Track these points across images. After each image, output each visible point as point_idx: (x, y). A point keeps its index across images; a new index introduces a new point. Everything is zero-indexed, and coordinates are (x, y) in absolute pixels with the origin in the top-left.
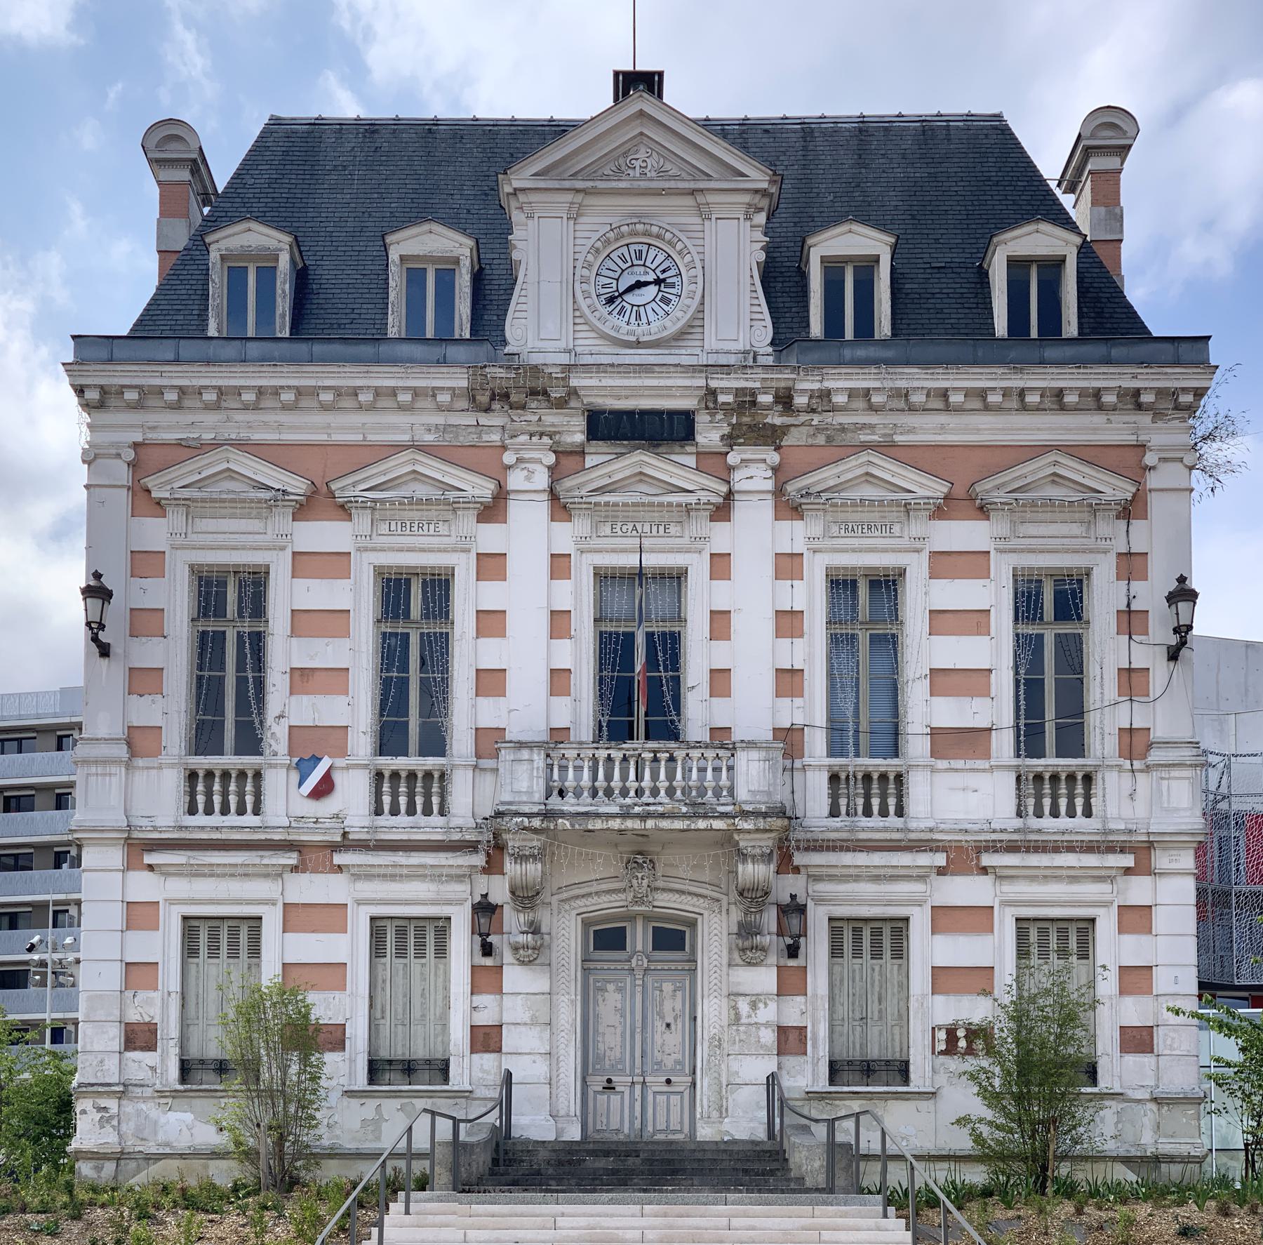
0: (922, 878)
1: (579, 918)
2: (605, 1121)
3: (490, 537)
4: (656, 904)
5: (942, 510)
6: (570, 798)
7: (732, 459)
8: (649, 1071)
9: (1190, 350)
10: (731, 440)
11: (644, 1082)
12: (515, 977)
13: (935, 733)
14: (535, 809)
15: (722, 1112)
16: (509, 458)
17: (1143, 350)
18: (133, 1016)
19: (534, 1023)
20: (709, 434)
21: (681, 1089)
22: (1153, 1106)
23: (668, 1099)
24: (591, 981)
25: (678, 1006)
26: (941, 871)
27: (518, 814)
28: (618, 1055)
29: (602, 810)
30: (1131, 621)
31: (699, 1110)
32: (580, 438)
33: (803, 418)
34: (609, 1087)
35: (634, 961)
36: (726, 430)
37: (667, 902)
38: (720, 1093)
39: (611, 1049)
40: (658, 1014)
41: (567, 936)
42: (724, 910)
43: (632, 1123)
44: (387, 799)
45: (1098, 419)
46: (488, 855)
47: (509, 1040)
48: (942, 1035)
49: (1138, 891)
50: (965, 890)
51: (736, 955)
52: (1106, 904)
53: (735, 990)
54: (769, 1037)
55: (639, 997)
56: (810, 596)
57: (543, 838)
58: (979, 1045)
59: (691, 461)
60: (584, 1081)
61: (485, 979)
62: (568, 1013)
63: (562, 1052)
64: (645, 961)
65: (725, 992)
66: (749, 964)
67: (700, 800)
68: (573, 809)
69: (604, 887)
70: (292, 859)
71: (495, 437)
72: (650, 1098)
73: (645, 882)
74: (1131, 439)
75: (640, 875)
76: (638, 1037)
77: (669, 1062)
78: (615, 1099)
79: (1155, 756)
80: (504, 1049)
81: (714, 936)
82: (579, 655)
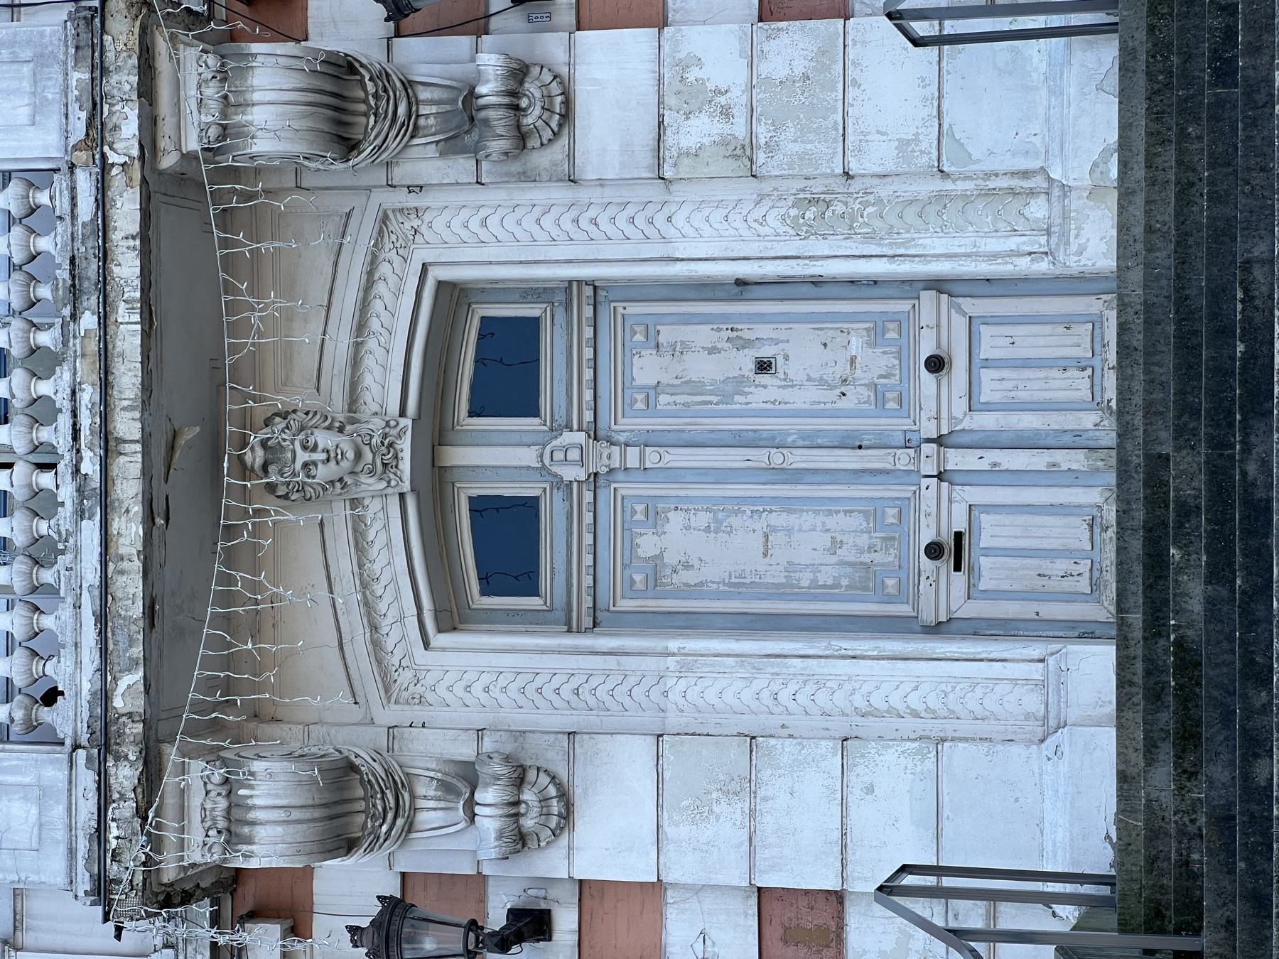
1: (439, 640)
2: (1062, 566)
4: (394, 407)
6: (58, 671)
8: (906, 424)
11: (939, 441)
14: (87, 779)
15: (1030, 183)
19: (749, 786)
21: (960, 324)
23: (987, 364)
24: (626, 604)
25: (702, 335)
27: (100, 832)
28: (856, 521)
29: (91, 576)
31: (1024, 265)
34: (953, 551)
35: (572, 473)
37: (388, 380)
38: (966, 198)
39: (836, 545)
40: (727, 398)
41: (480, 681)
42: (412, 201)
43: (1074, 478)
46: (255, 915)
51: (542, 159)
53: (645, 158)
55: (677, 458)
57: (172, 754)
60: (937, 629)
62: (718, 678)
63: (839, 699)
64: (567, 438)
65: (655, 192)
66: (567, 116)
67: (63, 274)
68: (90, 658)
69: (344, 565)
72: (986, 421)
73: (324, 439)
75: (302, 457)
76: (798, 459)
77: (876, 362)
78: (990, 533)
80: (832, 884)
81: (484, 230)
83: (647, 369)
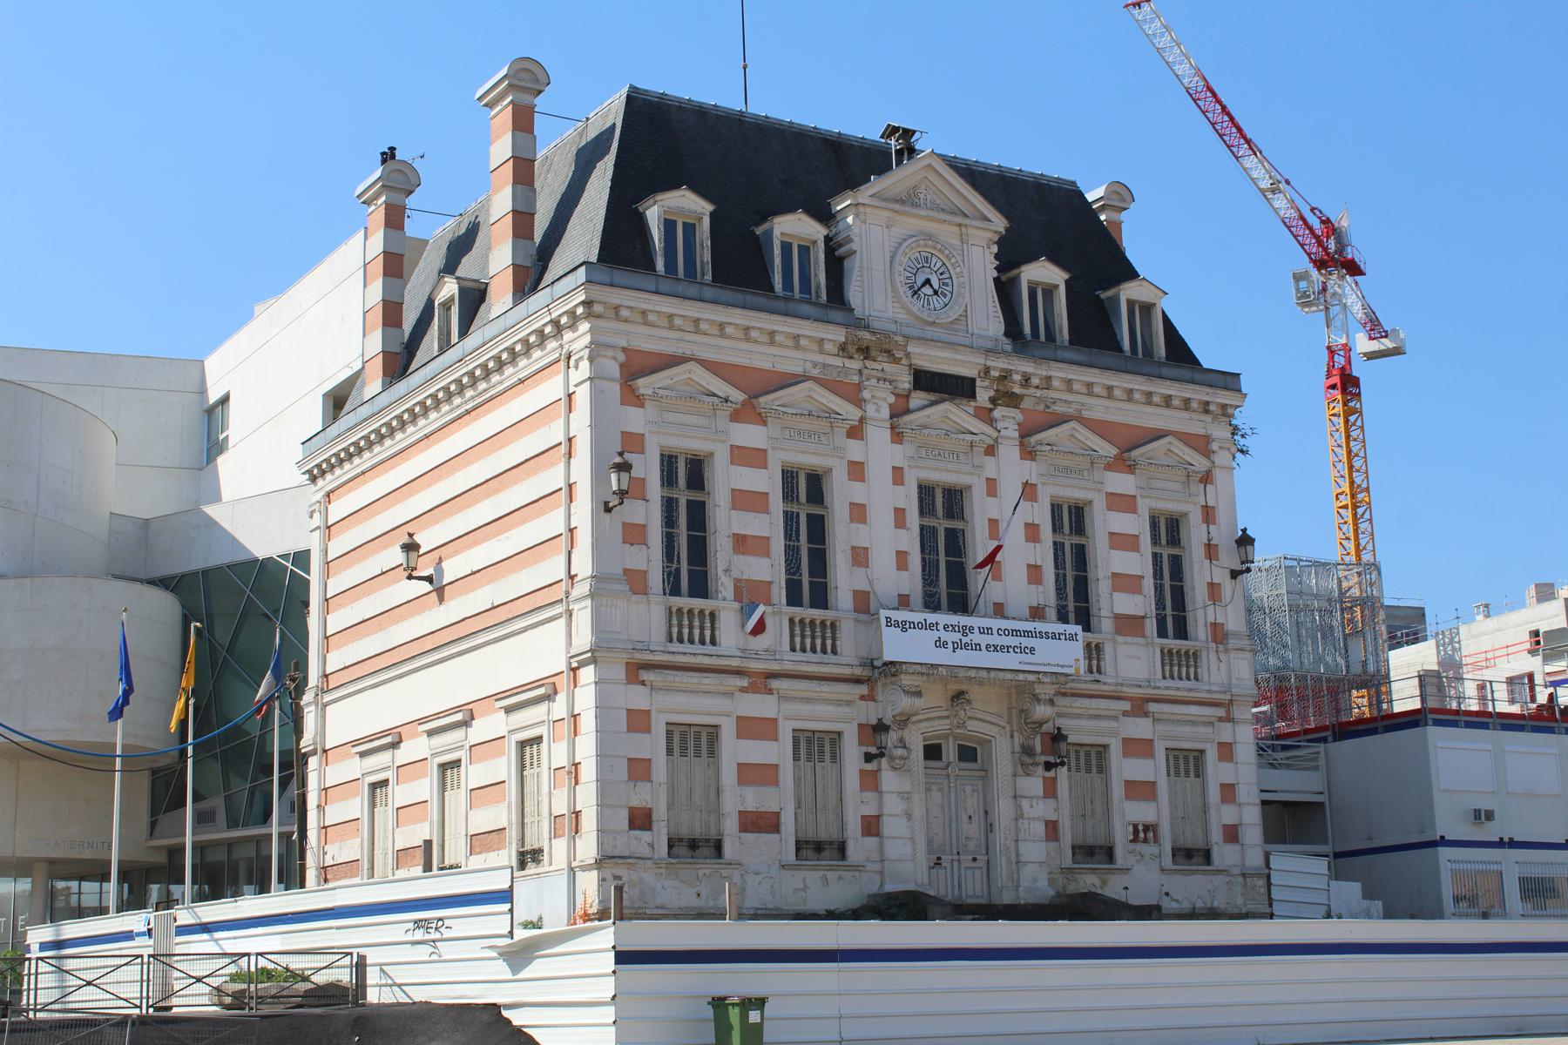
0: (1115, 718)
3: (854, 450)
5: (1112, 466)
7: (997, 413)
9: (1229, 381)
10: (993, 400)
12: (889, 780)
13: (1117, 617)
16: (866, 394)
17: (1198, 376)
18: (635, 803)
20: (983, 395)
22: (1240, 879)
26: (1125, 714)
30: (1211, 551)
32: (907, 386)
33: (1031, 391)
36: (992, 393)
44: (798, 640)
45: (1186, 415)
47: (889, 826)
48: (1131, 829)
49: (1225, 733)
50: (1140, 728)
52: (1211, 742)
54: (1040, 829)
56: (1041, 514)
58: (1151, 835)
59: (971, 410)
61: (870, 781)
70: (744, 682)
71: (856, 379)
74: (1202, 432)
77: (972, 845)
78: (942, 872)
79: (1232, 643)
81: (1003, 753)
82: (910, 541)
83: (969, 789)
